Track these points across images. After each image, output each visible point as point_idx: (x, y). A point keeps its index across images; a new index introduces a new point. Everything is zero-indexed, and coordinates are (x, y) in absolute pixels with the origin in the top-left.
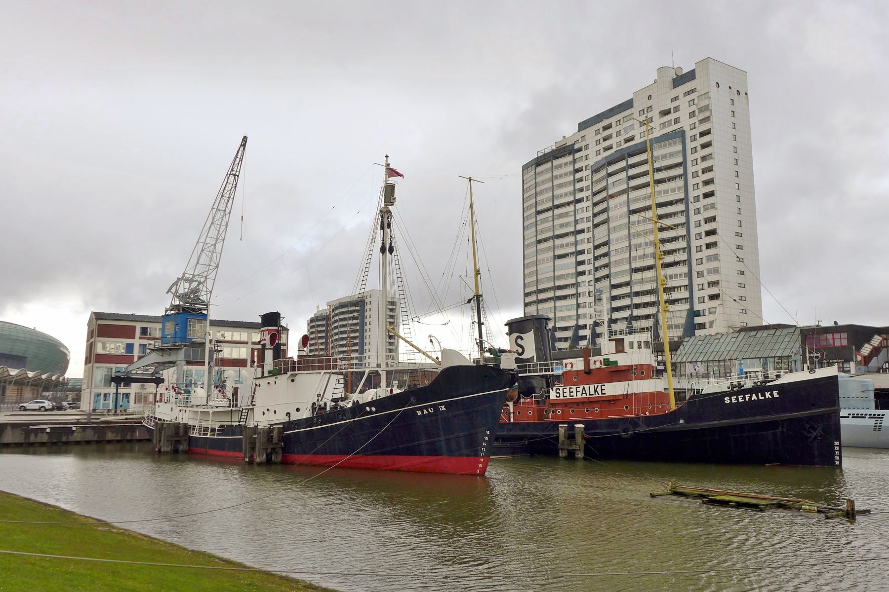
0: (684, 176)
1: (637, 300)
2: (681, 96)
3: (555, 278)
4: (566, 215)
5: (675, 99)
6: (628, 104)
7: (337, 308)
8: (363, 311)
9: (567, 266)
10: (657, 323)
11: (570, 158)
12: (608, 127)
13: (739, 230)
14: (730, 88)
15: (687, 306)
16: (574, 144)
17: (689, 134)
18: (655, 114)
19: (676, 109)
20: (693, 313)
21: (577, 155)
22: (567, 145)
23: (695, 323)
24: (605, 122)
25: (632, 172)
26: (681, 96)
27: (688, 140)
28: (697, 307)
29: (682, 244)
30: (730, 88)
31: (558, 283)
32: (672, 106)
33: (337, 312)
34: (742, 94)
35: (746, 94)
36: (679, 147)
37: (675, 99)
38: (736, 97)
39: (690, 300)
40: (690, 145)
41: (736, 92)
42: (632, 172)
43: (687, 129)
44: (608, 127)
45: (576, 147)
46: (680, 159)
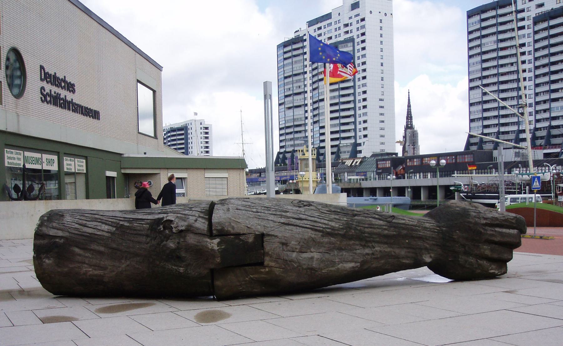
2: (353, 17)
3: (294, 120)
4: (299, 81)
5: (350, 18)
6: (328, 16)
7: (169, 132)
8: (186, 134)
9: (299, 112)
10: (339, 150)
12: (320, 28)
13: (382, 97)
14: (380, 12)
17: (357, 40)
18: (341, 25)
19: (351, 24)
20: (356, 145)
22: (300, 36)
23: (358, 150)
24: (319, 25)
26: (353, 17)
27: (356, 44)
28: (359, 141)
31: (296, 123)
32: (349, 22)
33: (169, 134)
34: (388, 15)
35: (391, 14)
37: (350, 18)
39: (355, 137)
40: (357, 47)
43: (355, 37)
44: (320, 28)
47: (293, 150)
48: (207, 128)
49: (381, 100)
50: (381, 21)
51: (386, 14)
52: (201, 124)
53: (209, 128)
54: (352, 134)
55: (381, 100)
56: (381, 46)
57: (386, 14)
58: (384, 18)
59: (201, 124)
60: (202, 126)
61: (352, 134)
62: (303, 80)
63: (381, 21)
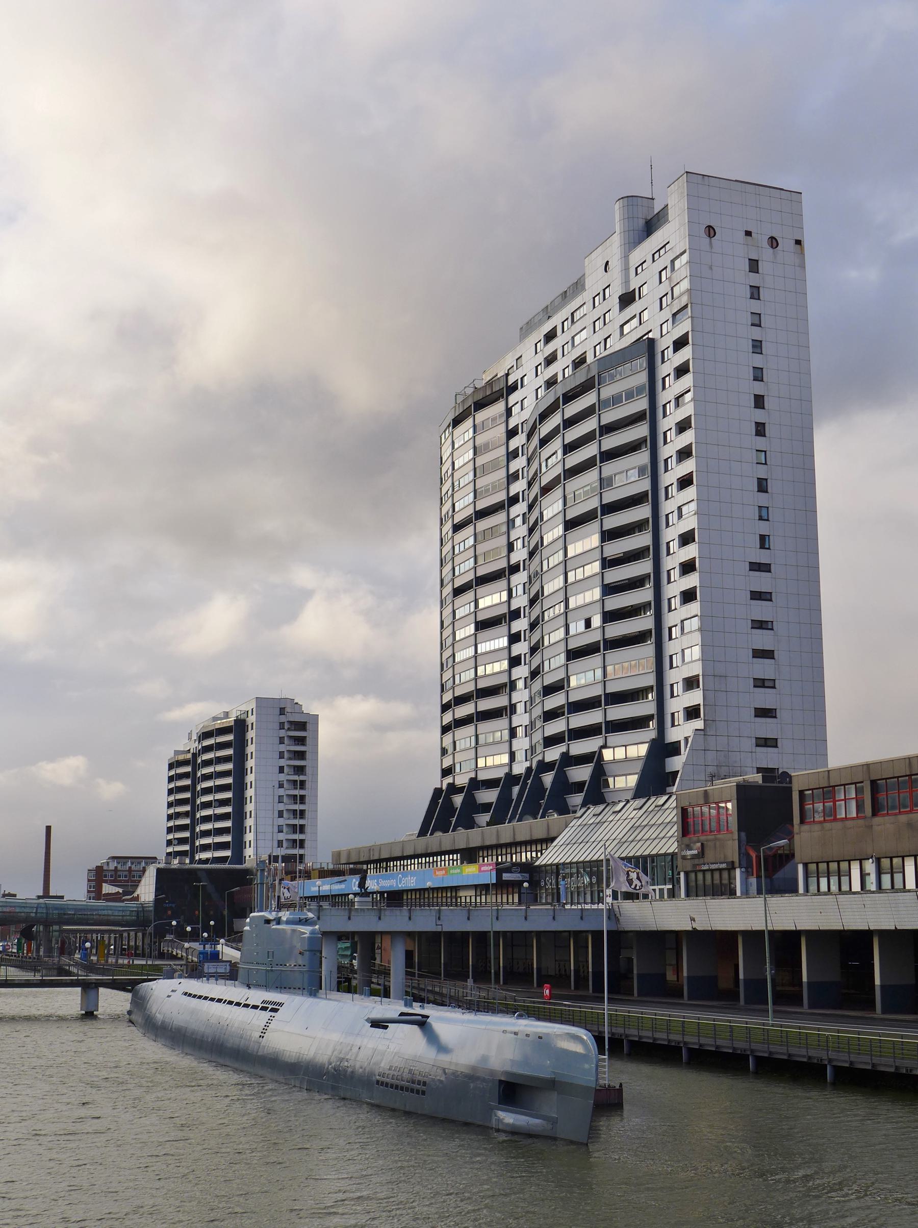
0: (652, 442)
1: (580, 720)
8: (240, 744)
11: (498, 408)
12: (550, 337)
13: (762, 557)
15: (650, 733)
16: (507, 375)
21: (513, 398)
25: (573, 434)
29: (644, 595)
30: (748, 233)
34: (786, 244)
35: (798, 242)
36: (642, 378)
38: (765, 255)
41: (765, 244)
42: (573, 434)
44: (550, 337)
45: (511, 380)
46: (642, 404)
47: (471, 779)
48: (302, 726)
49: (757, 567)
50: (754, 266)
51: (773, 242)
52: (282, 711)
53: (308, 726)
54: (646, 707)
55: (757, 567)
56: (758, 361)
57: (773, 242)
58: (765, 255)
59: (282, 711)
60: (283, 719)
61: (646, 707)
62: (504, 528)
63: (754, 266)
